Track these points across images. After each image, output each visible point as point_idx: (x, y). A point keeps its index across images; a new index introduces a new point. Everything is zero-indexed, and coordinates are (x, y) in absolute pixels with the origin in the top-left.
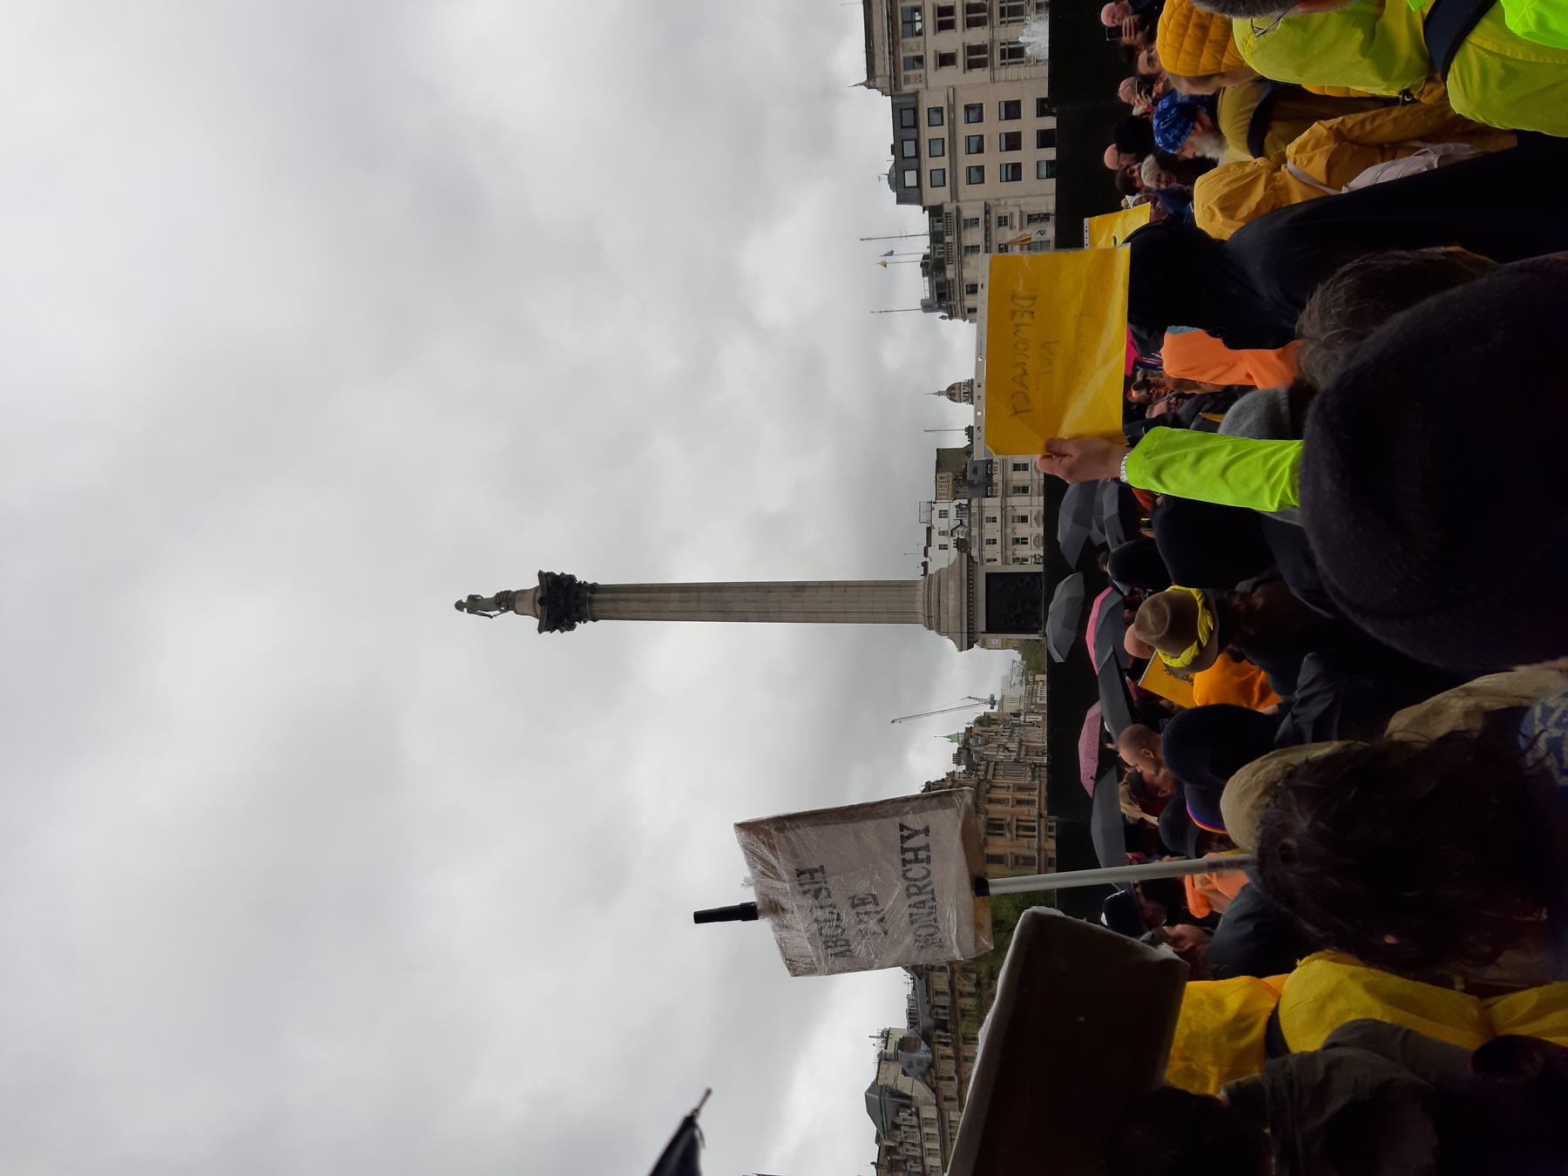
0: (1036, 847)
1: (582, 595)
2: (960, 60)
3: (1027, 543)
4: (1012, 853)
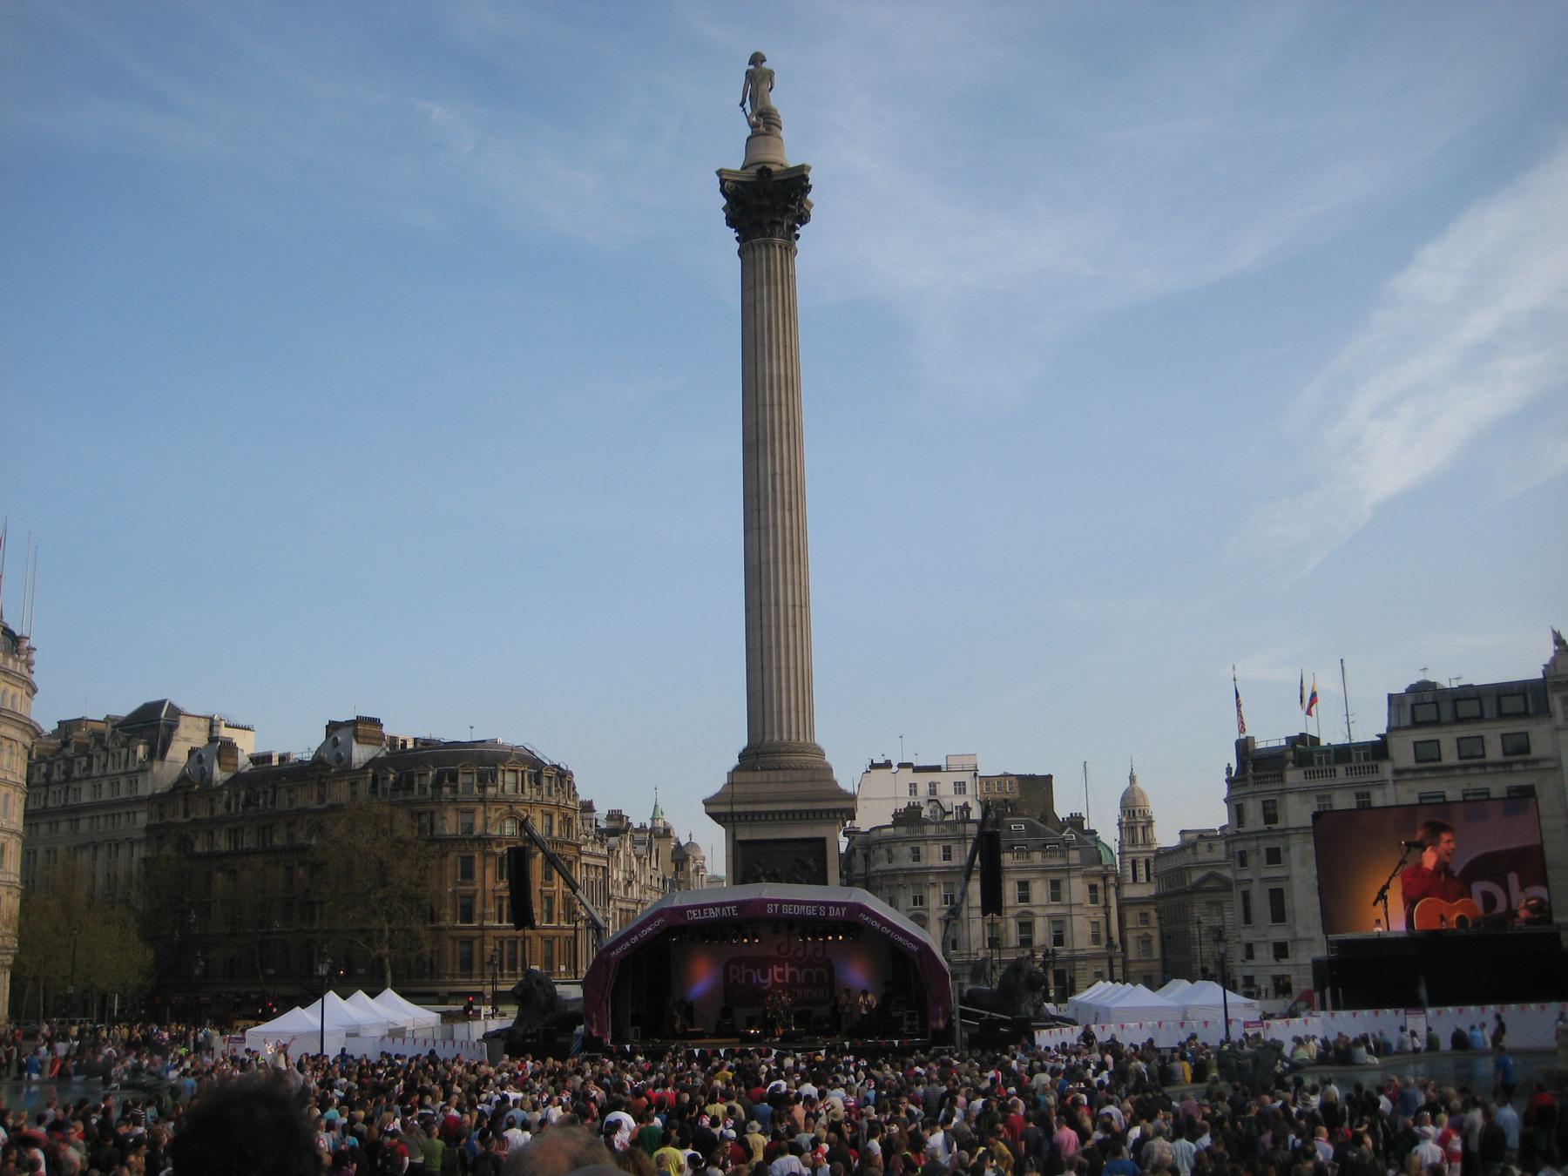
0: (486, 923)
1: (778, 228)
3: (915, 904)
4: (476, 891)
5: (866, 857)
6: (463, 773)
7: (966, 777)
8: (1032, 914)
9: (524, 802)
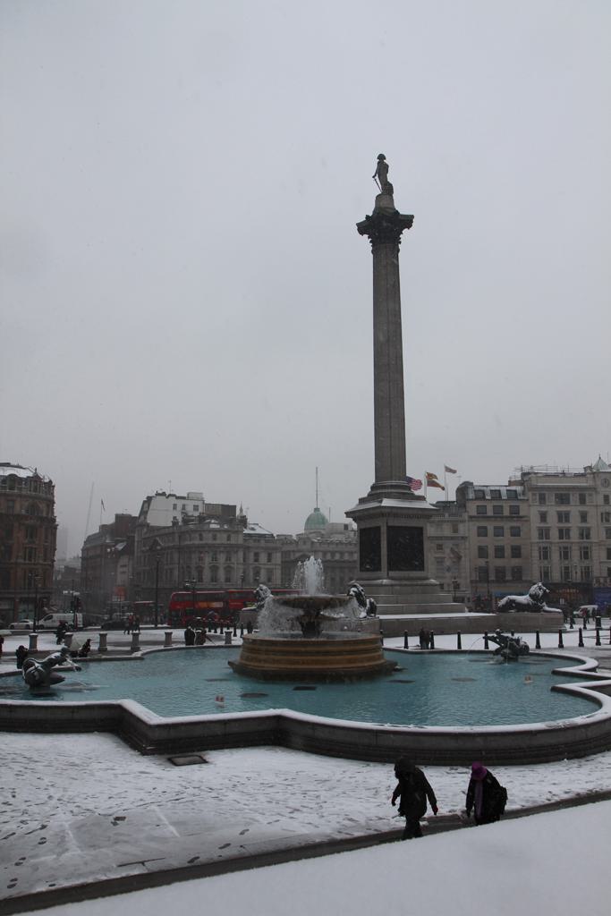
0: (21, 561)
2: (542, 525)
5: (180, 537)
7: (199, 503)
8: (260, 568)
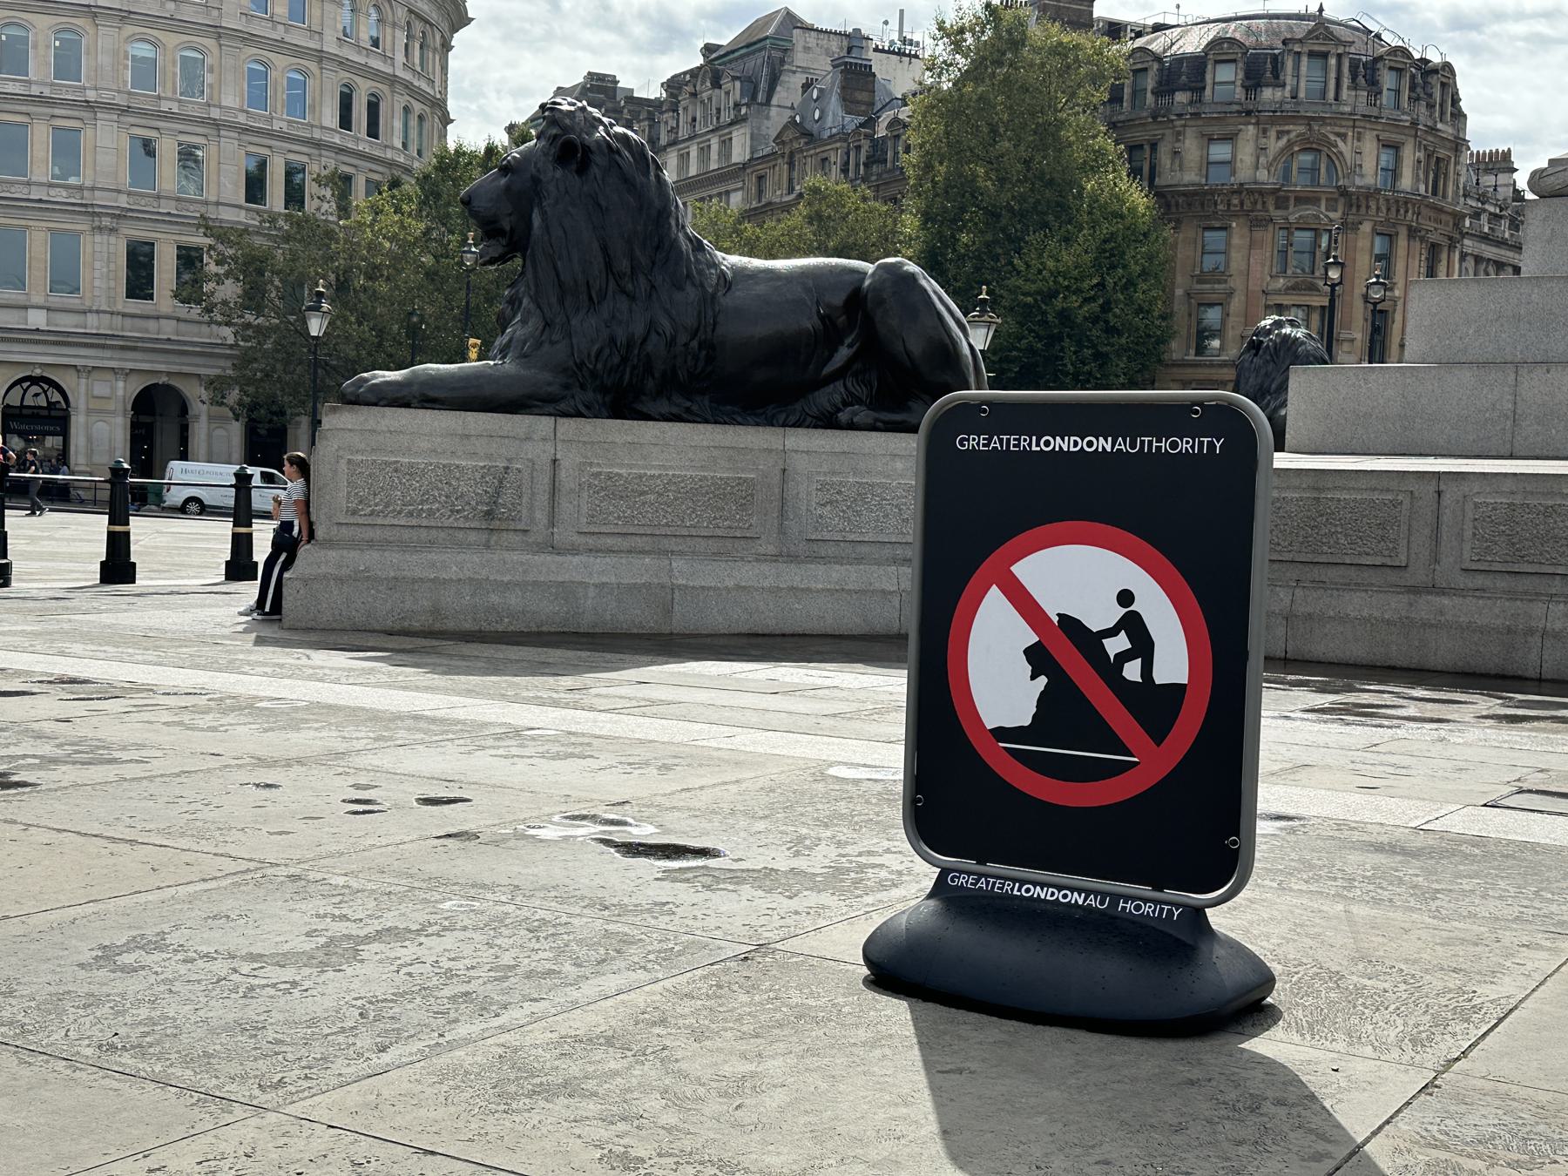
6: (1217, 62)
9: (1339, 118)
